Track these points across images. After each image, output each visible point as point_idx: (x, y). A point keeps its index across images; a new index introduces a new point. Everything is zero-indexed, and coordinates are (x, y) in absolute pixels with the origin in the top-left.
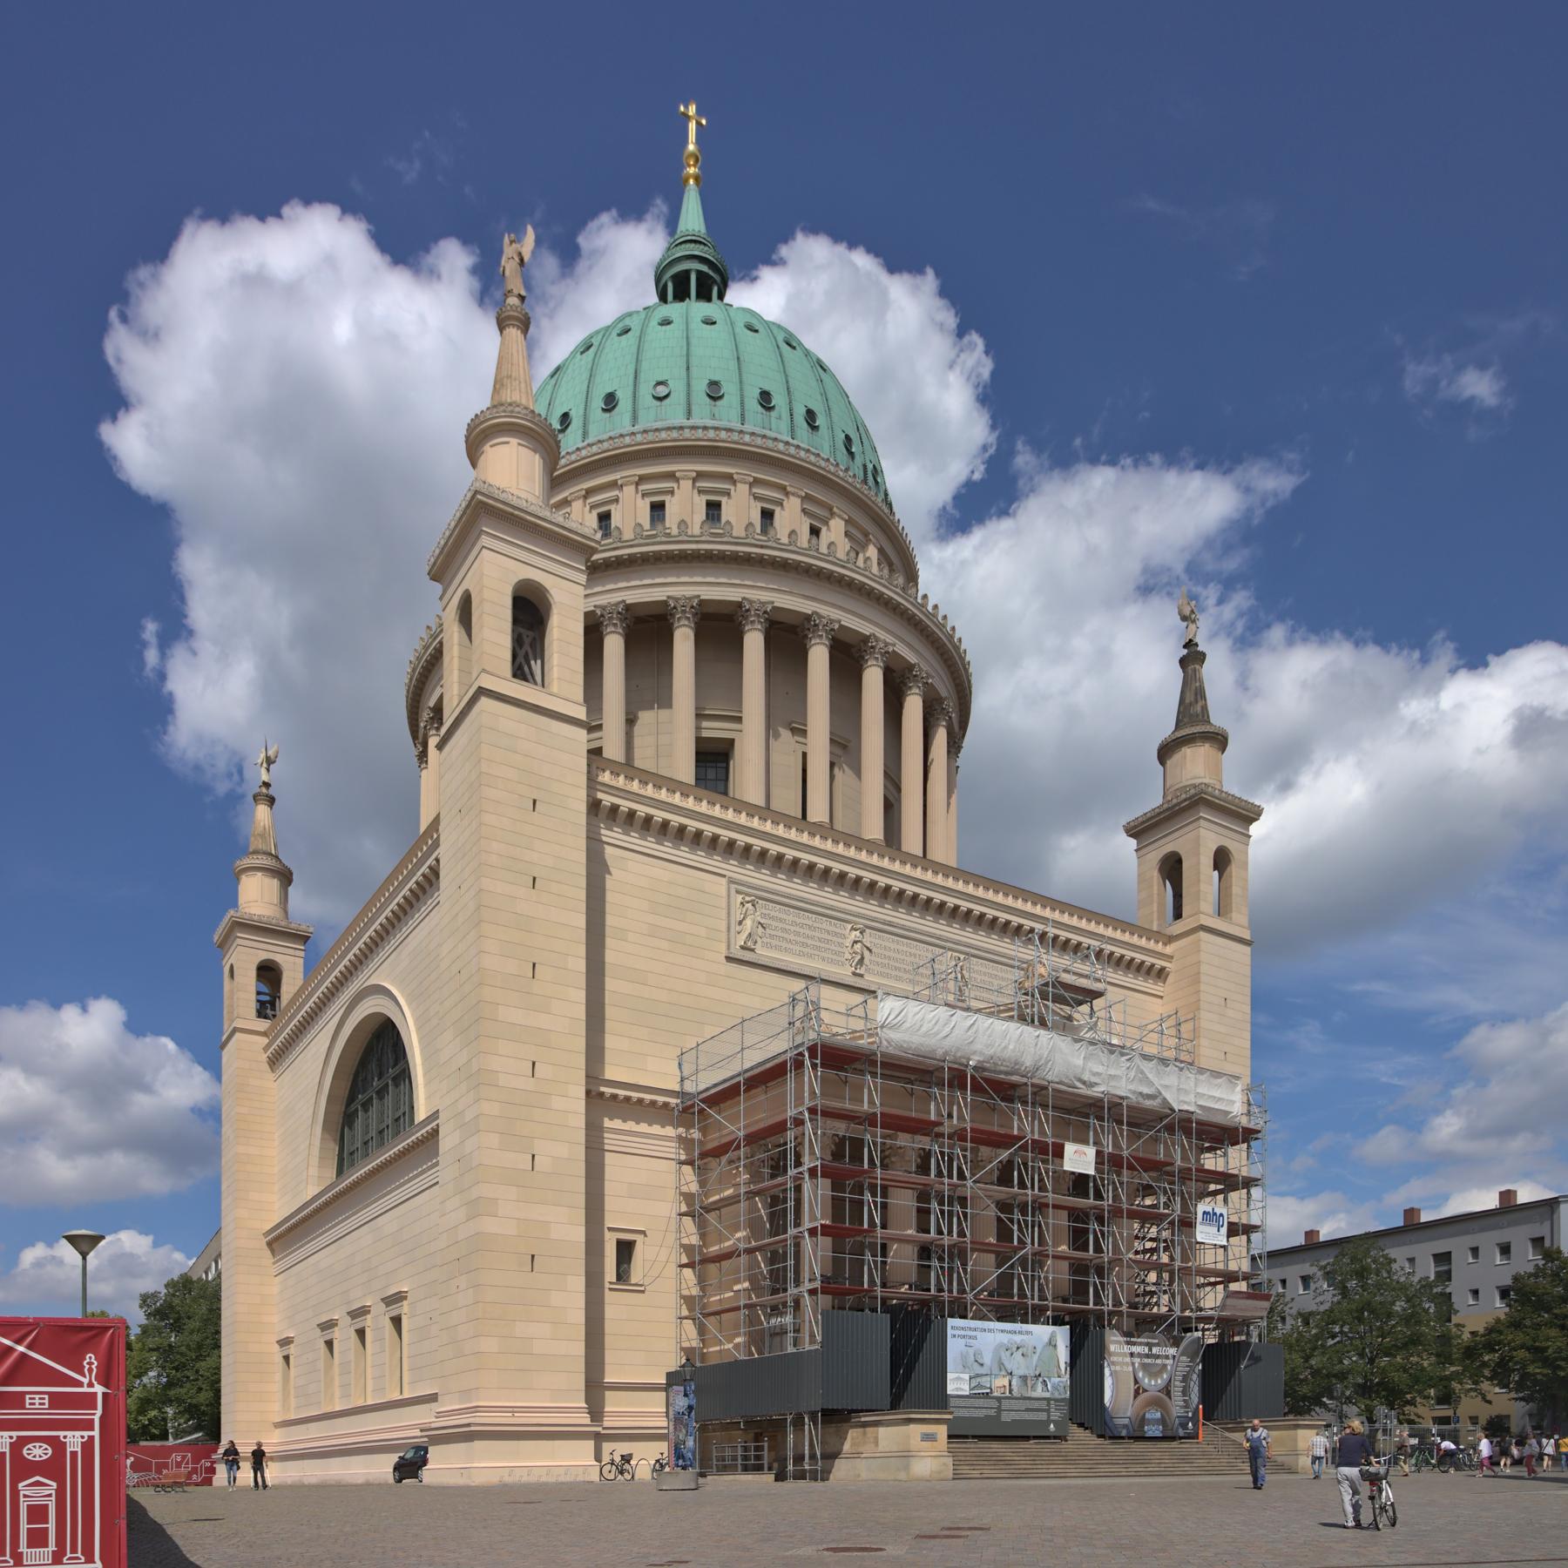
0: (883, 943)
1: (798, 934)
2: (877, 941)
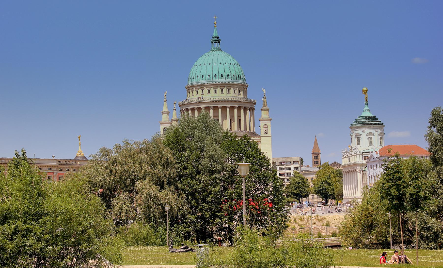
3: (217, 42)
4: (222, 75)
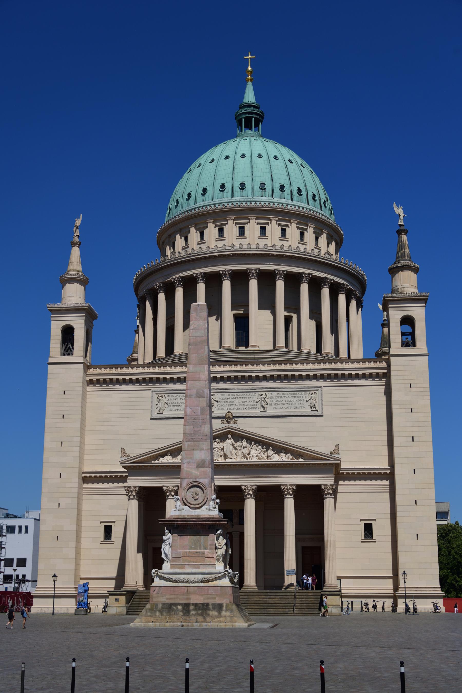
0: (224, 397)
2: (220, 397)
3: (254, 116)
4: (263, 184)
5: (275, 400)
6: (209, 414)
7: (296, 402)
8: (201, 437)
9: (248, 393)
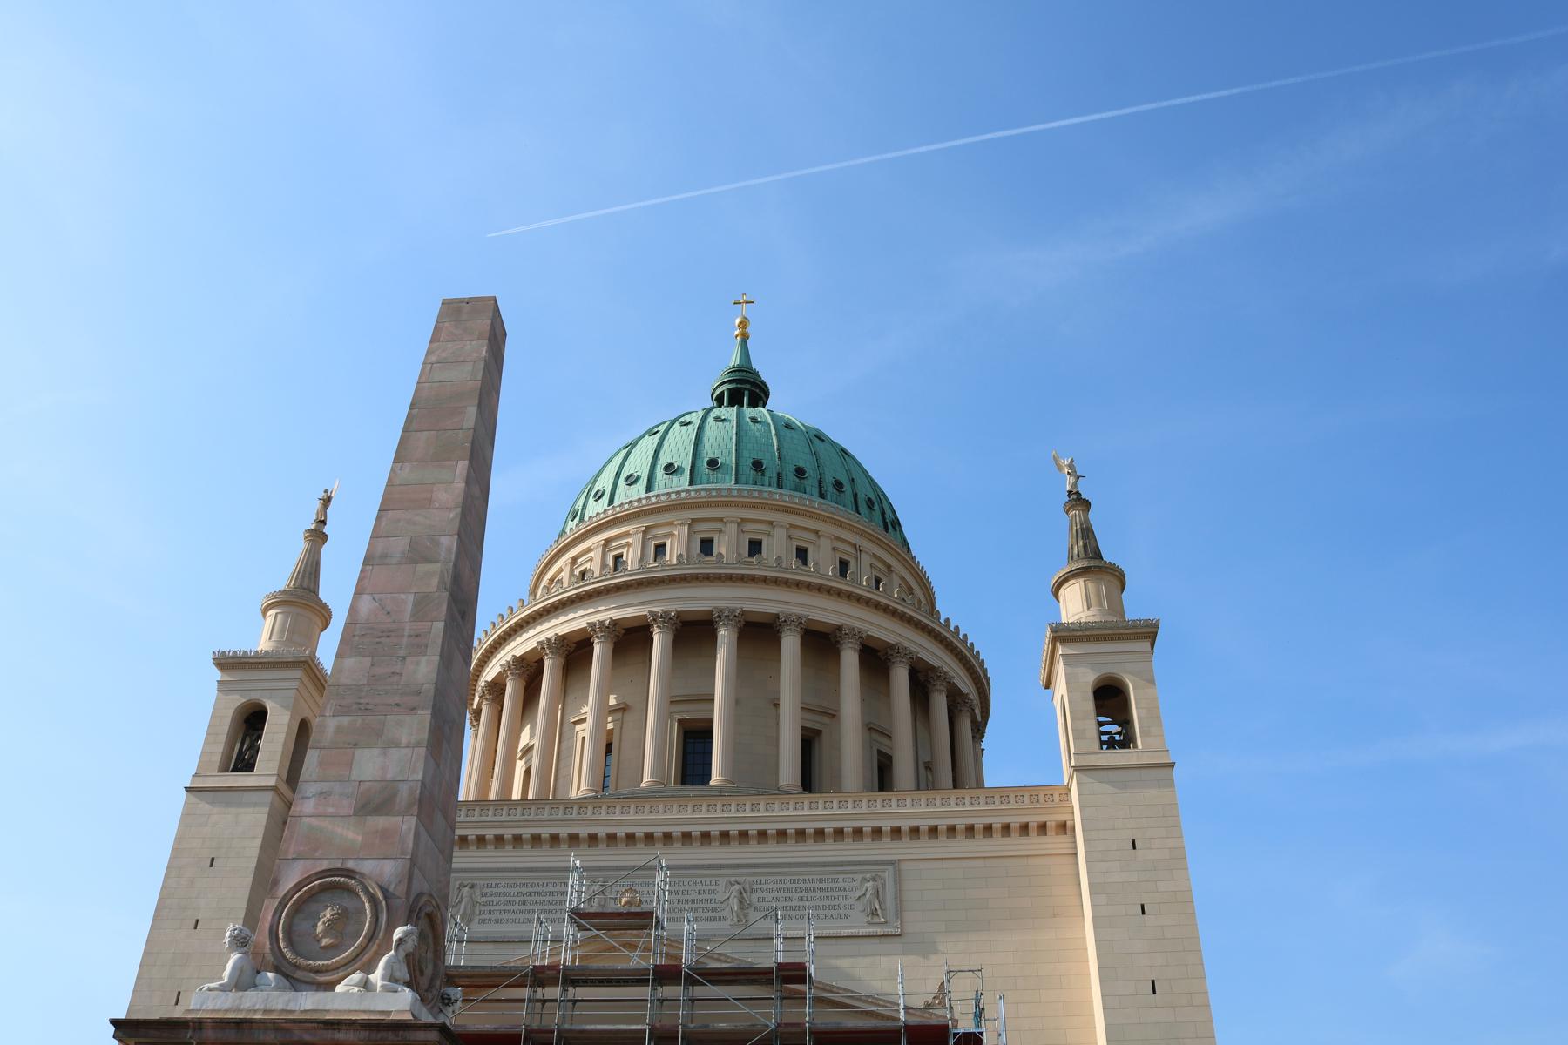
1: (524, 903)
3: (748, 386)
5: (770, 896)
6: (444, 618)
7: (827, 903)
8: (397, 699)
9: (699, 880)
